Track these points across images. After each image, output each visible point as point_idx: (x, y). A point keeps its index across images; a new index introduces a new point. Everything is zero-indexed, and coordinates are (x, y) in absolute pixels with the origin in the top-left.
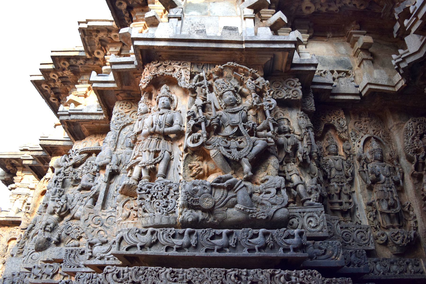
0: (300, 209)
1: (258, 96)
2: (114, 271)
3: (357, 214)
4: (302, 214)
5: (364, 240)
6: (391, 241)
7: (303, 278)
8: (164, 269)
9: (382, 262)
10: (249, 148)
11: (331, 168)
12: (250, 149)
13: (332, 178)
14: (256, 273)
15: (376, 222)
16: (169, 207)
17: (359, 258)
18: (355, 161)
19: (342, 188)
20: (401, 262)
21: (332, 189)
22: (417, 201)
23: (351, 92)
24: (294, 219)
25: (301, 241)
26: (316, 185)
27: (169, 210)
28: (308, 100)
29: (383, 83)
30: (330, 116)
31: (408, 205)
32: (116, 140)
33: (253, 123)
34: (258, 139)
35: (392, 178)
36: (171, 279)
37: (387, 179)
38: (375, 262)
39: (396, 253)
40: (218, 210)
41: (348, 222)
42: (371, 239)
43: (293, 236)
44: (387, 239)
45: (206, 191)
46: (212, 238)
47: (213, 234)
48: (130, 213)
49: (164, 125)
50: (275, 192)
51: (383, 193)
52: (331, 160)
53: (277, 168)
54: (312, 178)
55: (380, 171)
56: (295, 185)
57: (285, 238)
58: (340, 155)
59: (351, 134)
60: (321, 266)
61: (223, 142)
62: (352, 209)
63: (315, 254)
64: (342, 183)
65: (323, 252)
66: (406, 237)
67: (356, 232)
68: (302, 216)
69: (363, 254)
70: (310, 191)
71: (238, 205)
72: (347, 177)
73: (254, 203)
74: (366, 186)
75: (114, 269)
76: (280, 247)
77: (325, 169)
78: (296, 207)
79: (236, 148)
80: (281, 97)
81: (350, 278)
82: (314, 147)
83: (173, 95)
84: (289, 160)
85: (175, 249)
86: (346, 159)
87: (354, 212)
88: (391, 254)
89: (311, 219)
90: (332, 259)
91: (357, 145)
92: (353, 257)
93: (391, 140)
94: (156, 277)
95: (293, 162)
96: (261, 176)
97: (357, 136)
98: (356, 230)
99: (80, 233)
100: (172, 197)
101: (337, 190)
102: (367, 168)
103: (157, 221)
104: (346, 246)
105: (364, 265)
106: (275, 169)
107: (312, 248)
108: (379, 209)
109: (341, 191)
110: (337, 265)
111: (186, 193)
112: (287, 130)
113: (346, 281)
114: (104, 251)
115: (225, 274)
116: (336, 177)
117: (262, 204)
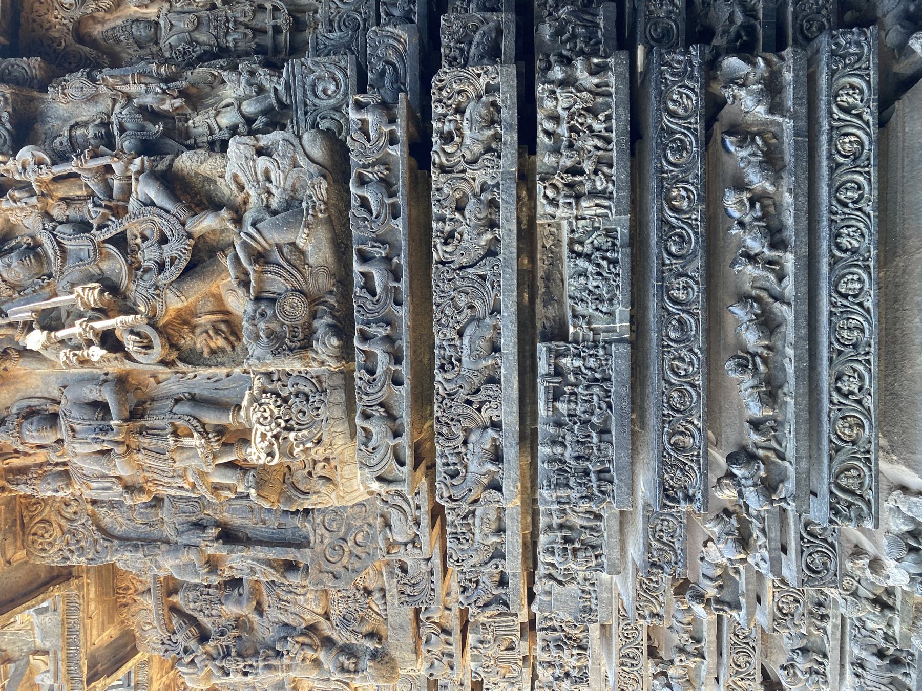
2: (445, 484)
4: (309, 108)
7: (447, 106)
8: (437, 386)
10: (160, 216)
11: (192, 41)
12: (163, 213)
14: (439, 201)
16: (307, 390)
19: (241, 23)
21: (242, 45)
26: (240, 74)
27: (314, 390)
28: (10, 73)
30: (50, 27)
32: (139, 543)
33: (90, 206)
34: (134, 194)
36: (456, 369)
40: (311, 287)
43: (364, 122)
45: (269, 312)
46: (373, 293)
47: (364, 290)
48: (320, 476)
49: (103, 423)
50: (267, 158)
52: (173, 40)
53: (207, 155)
54: (223, 82)
56: (242, 120)
57: (369, 140)
58: (158, 17)
60: (417, 74)
61: (146, 277)
63: (395, 86)
64: (228, 21)
65: (391, 68)
68: (313, 108)
70: (254, 88)
71: (297, 241)
73: (292, 204)
75: (443, 486)
78: (294, 122)
79: (160, 246)
81: (442, 17)
83: (14, 410)
84: (179, 130)
85: (398, 367)
89: (320, 88)
90: (405, 50)
92: (397, 13)
94: (452, 400)
95: (187, 122)
96: (226, 191)
99: (357, 593)
100: (284, 386)
101: (246, 35)
103: (338, 412)
106: (210, 160)
109: (247, 26)
110: (415, 40)
111: (275, 353)
114: (402, 517)
115: (443, 263)
117: (294, 190)
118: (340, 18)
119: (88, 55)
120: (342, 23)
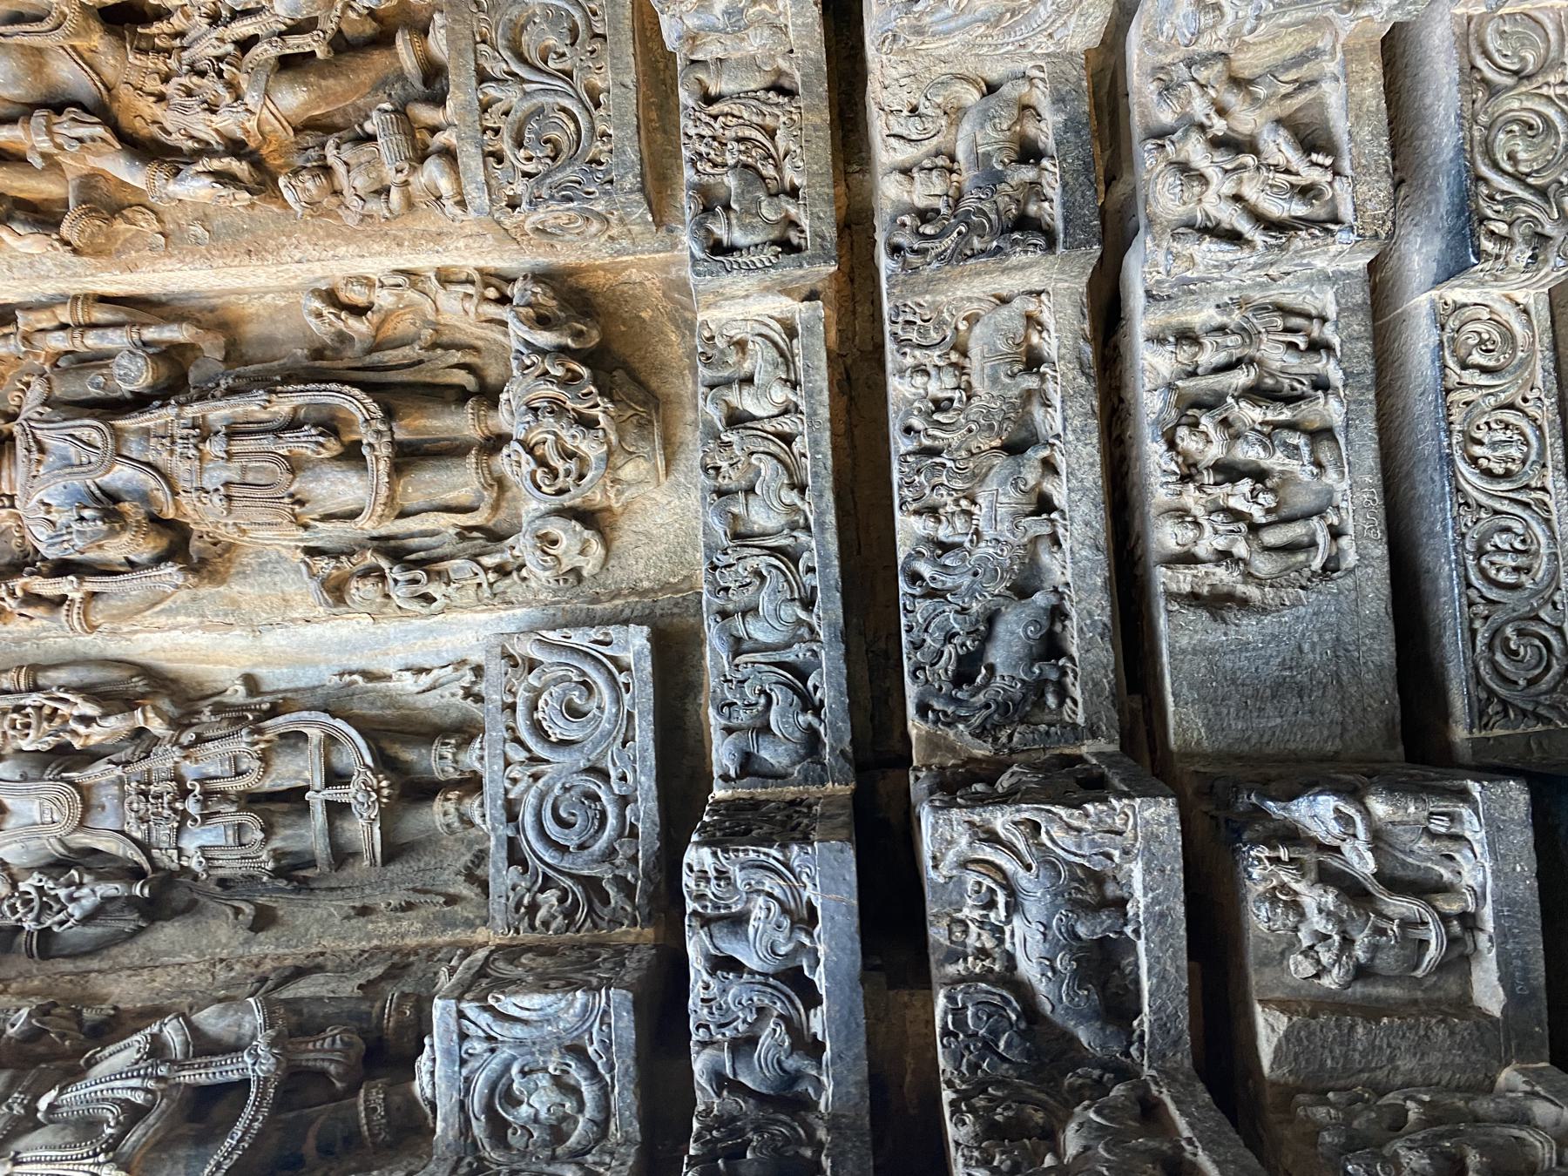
3: (408, 684)
13: (150, 859)
19: (224, 795)
20: (724, 465)
21: (230, 866)
22: (298, 256)
31: (327, 311)
38: (737, 646)
39: (661, 463)
51: (246, 491)
64: (184, 793)
66: (553, 391)
67: (539, 750)
77: (75, 910)
87: (392, 701)
101: (240, 828)
116: (138, 835)
118: (542, 797)
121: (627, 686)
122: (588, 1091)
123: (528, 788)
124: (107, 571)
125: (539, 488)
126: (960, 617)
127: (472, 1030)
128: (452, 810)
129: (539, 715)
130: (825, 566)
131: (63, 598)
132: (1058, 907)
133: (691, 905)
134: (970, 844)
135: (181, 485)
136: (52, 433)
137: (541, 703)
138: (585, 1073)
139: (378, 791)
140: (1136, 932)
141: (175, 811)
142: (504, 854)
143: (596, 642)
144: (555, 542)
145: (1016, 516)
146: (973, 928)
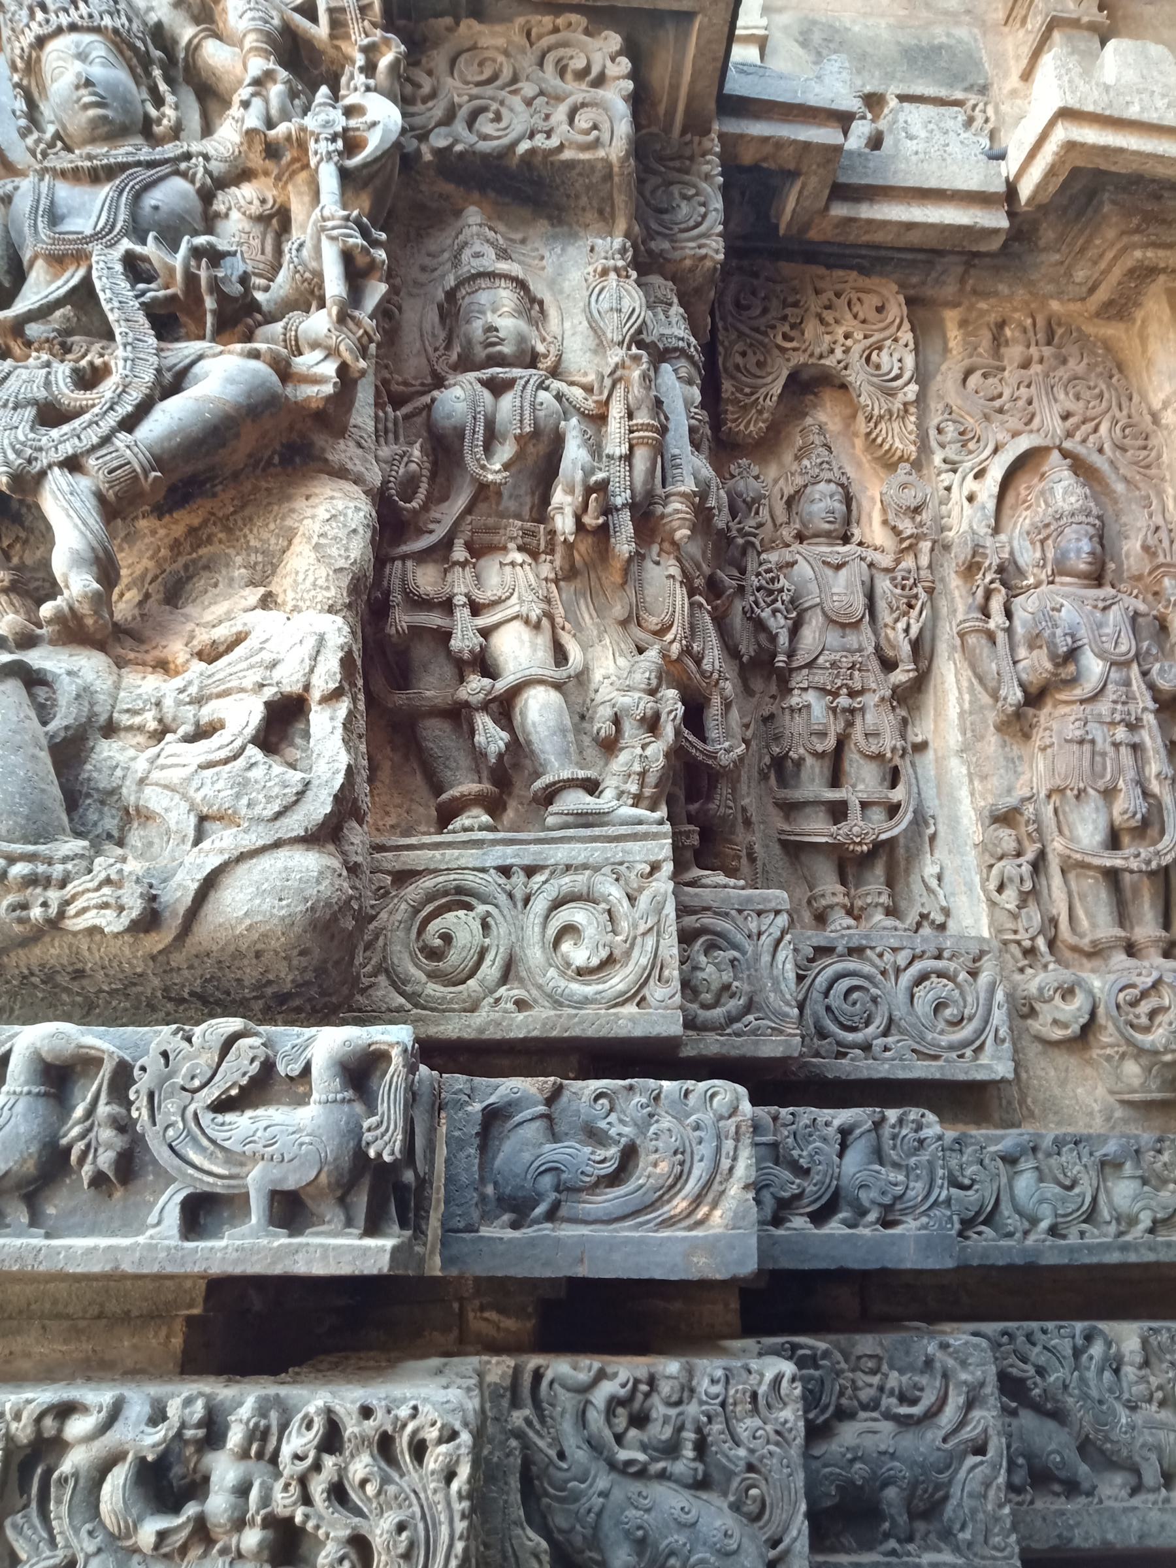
0: (510, 850)
1: (283, 74)
4: (519, 878)
5: (958, 1023)
6: (1111, 1028)
9: (1053, 1161)
15: (1033, 916)
17: (896, 1166)
18: (942, 580)
19: (850, 724)
21: (795, 726)
23: (961, 184)
24: (461, 913)
25: (356, 1132)
26: (652, 692)
29: (1152, 117)
35: (1145, 674)
37: (1115, 675)
38: (1010, 1160)
39: (1137, 1097)
41: (870, 916)
42: (999, 1017)
44: (1093, 1014)
51: (1088, 755)
52: (804, 569)
53: (341, 563)
55: (1083, 632)
56: (501, 685)
57: (222, 1106)
58: (860, 544)
59: (940, 431)
62: (902, 841)
64: (852, 694)
65: (609, 1168)
67: (906, 978)
68: (519, 895)
69: (921, 1142)
72: (889, 665)
74: (992, 717)
76: (174, 1180)
77: (766, 614)
79: (35, 402)
80: (495, 143)
82: (678, 466)
84: (493, 530)
86: (891, 565)
87: (913, 857)
88: (1111, 1099)
91: (965, 493)
93: (1159, 467)
95: (520, 549)
97: (971, 445)
98: (910, 963)
101: (823, 735)
102: (1009, 614)
104: (845, 1055)
105: (924, 1213)
107: (532, 1131)
108: (1057, 845)
112: (506, 349)
113: (754, 1395)
116: (821, 660)
118: (867, 977)
119: (763, 390)
120: (855, 982)
121: (961, 1056)
122: (718, 1013)
123: (877, 967)
124: (1012, 649)
125: (1121, 990)
126: (1060, 1384)
127: (767, 919)
128: (836, 900)
129: (934, 978)
130: (1090, 1248)
131: (988, 616)
132: (911, 1469)
133: (892, 1114)
134: (965, 1383)
135: (1089, 707)
136: (1119, 618)
137: (945, 981)
138: (734, 1013)
139: (860, 843)
140: (893, 1553)
141: (839, 688)
142: (823, 943)
143: (997, 1031)
144: (1063, 998)
145: (1158, 1449)
146: (875, 1380)
